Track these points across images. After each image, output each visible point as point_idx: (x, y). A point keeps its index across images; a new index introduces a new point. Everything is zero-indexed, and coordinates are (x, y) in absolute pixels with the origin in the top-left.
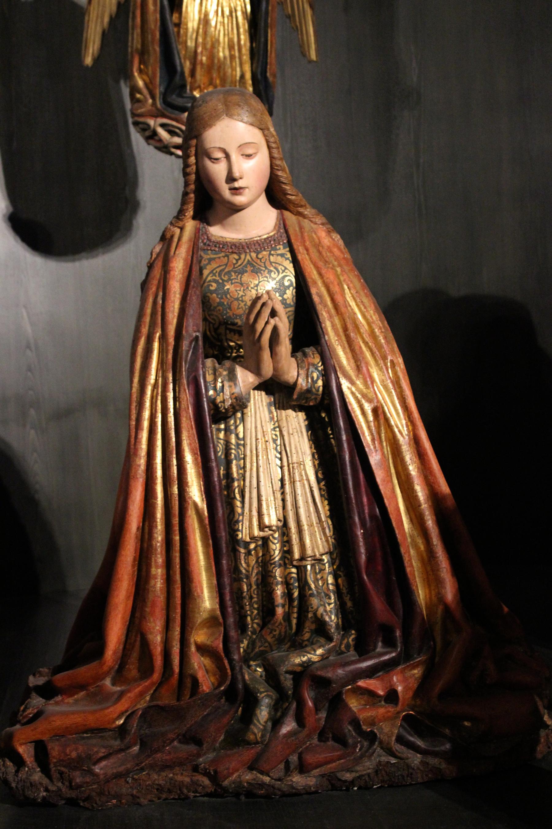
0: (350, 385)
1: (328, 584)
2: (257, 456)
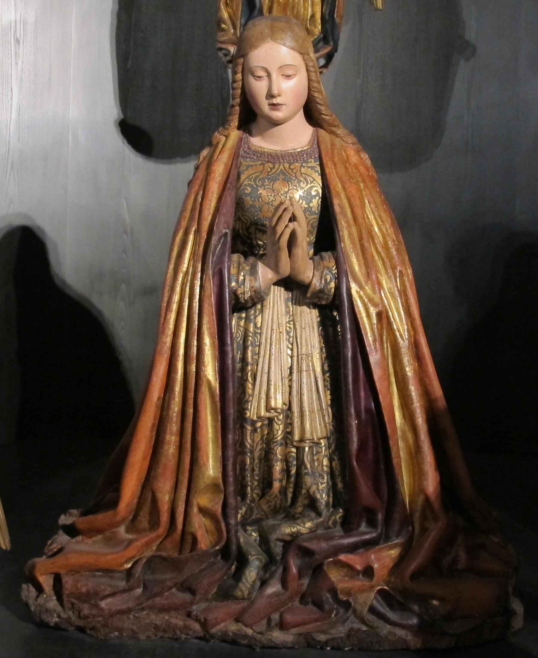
0: (358, 290)
1: (322, 465)
2: (271, 345)
